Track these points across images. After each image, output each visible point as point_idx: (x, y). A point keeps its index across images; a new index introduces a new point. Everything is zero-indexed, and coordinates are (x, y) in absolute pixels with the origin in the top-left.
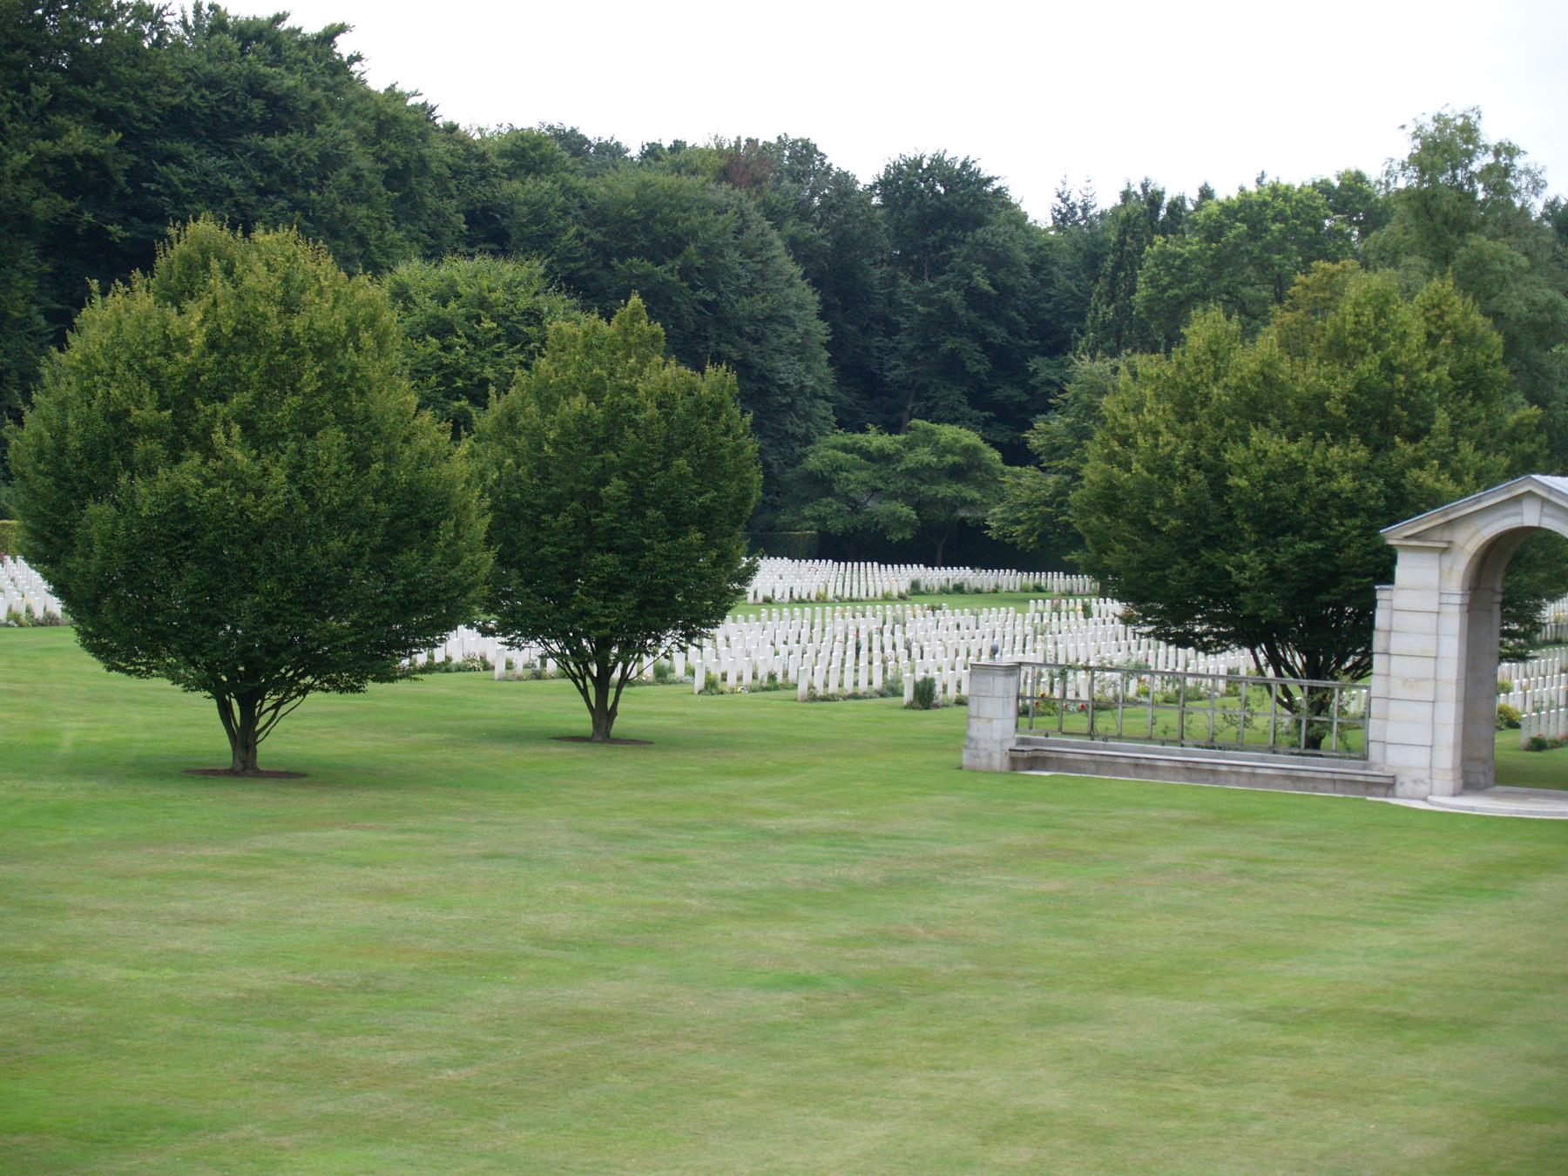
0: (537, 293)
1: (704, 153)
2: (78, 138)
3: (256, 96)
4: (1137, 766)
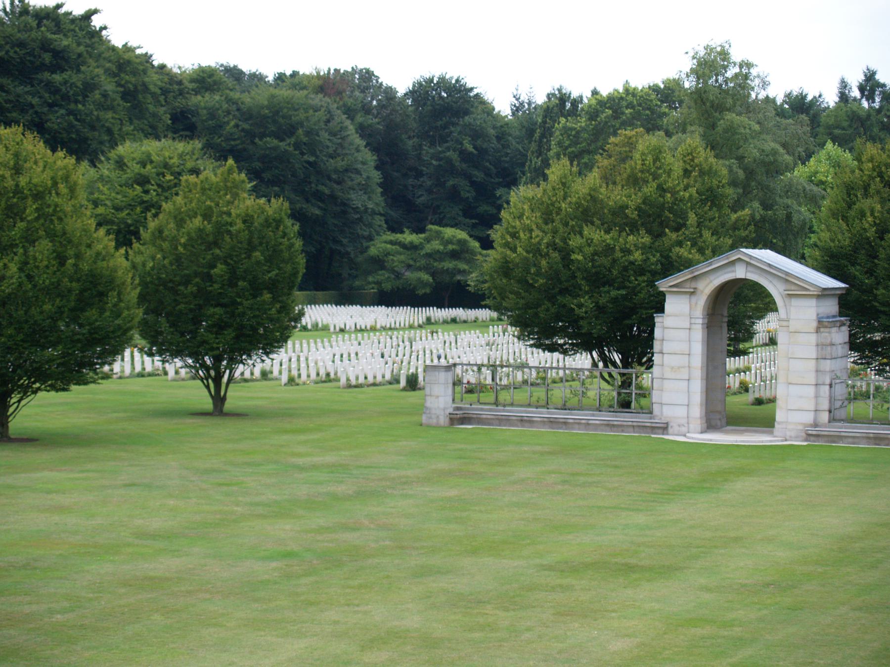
0: (197, 159)
1: (309, 78)
3: (46, 51)
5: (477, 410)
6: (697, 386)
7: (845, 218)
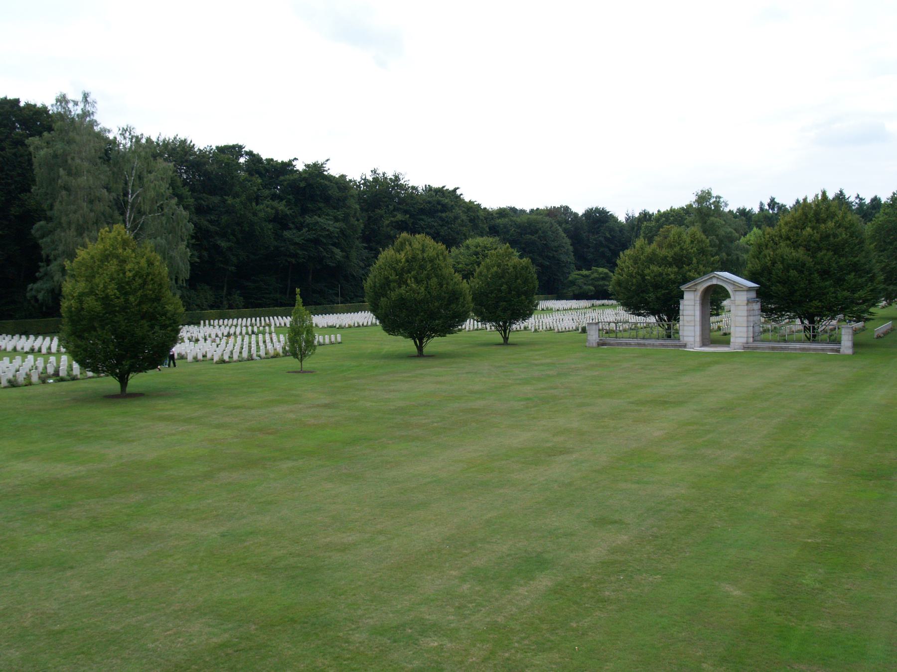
2: (399, 217)
4: (627, 344)
5: (609, 340)
6: (698, 329)
7: (758, 258)
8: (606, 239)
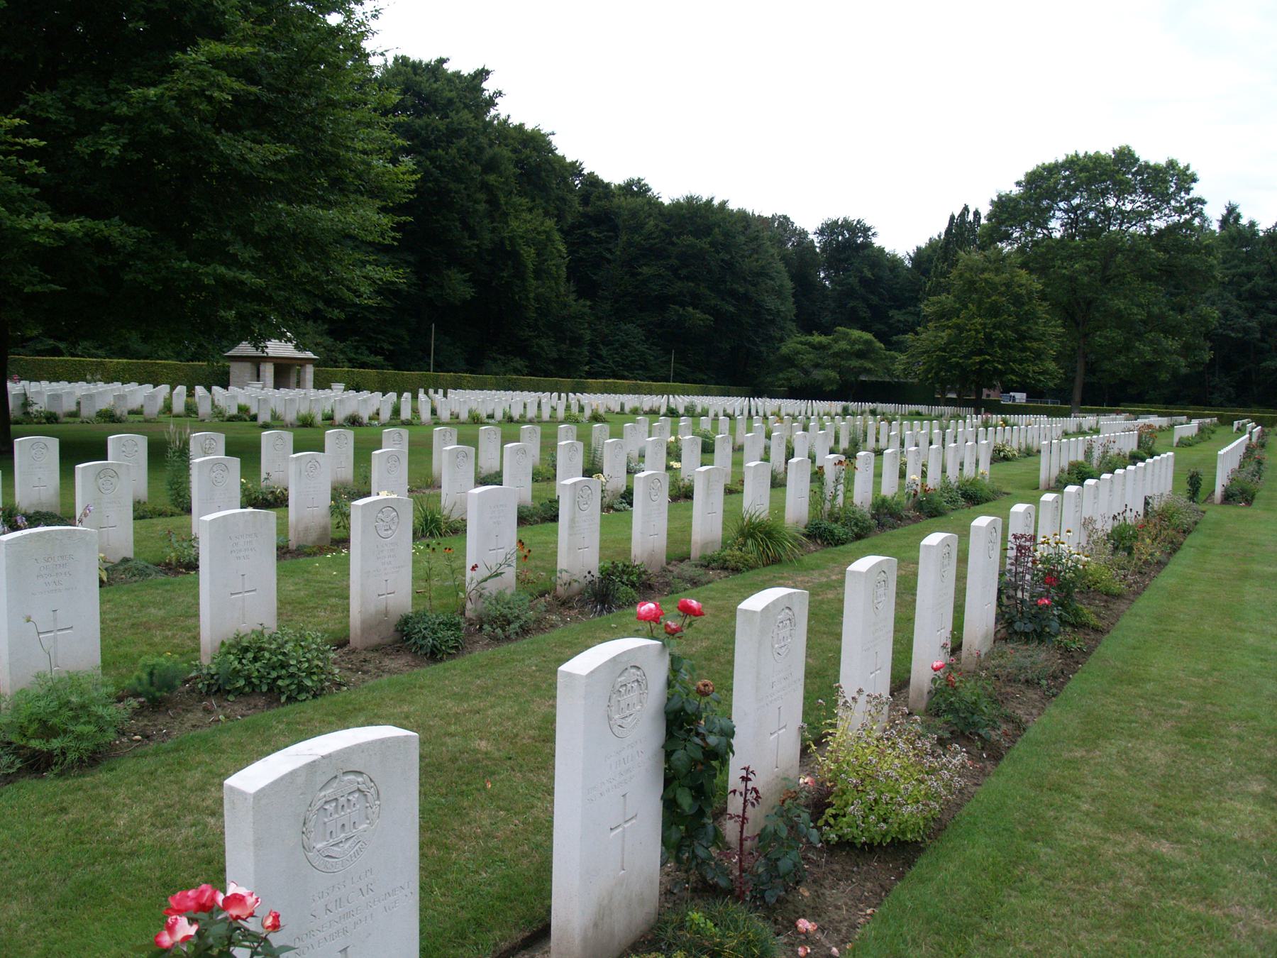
8: (863, 281)
